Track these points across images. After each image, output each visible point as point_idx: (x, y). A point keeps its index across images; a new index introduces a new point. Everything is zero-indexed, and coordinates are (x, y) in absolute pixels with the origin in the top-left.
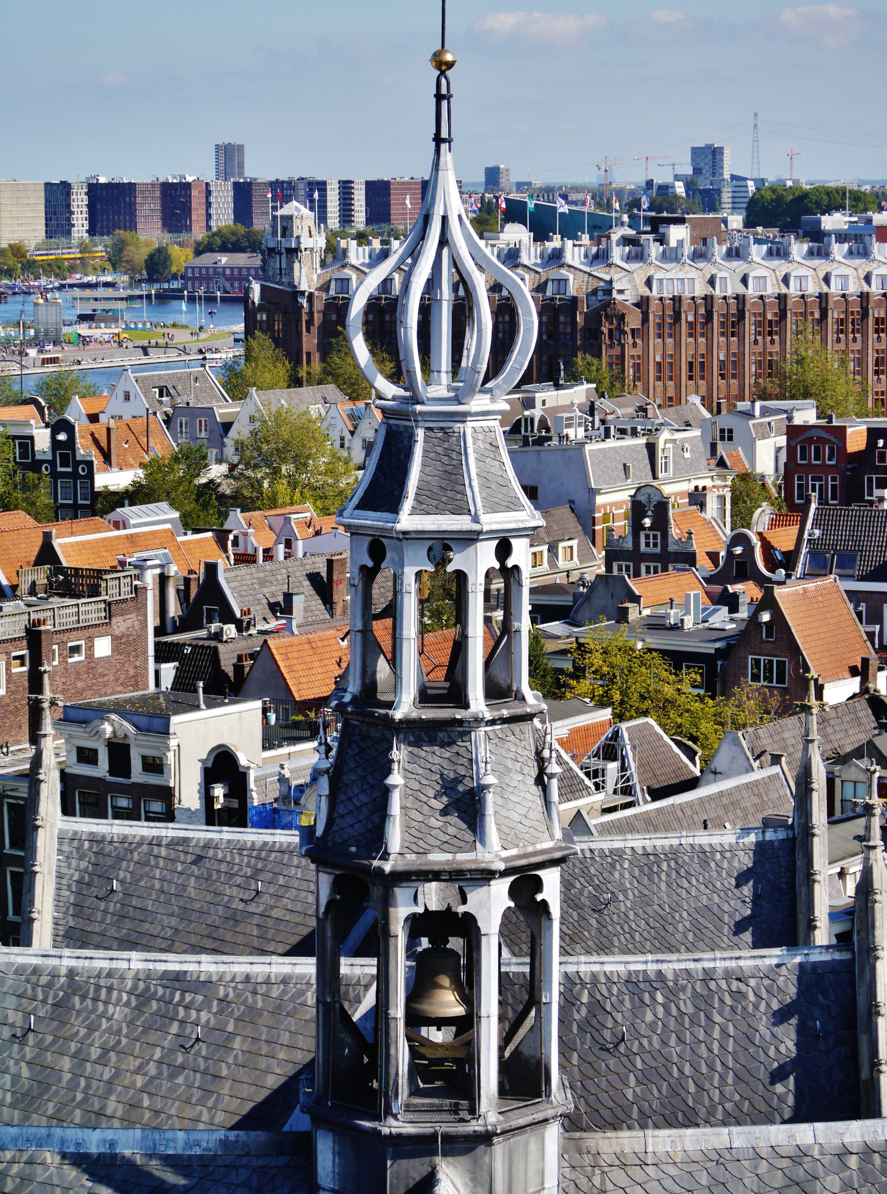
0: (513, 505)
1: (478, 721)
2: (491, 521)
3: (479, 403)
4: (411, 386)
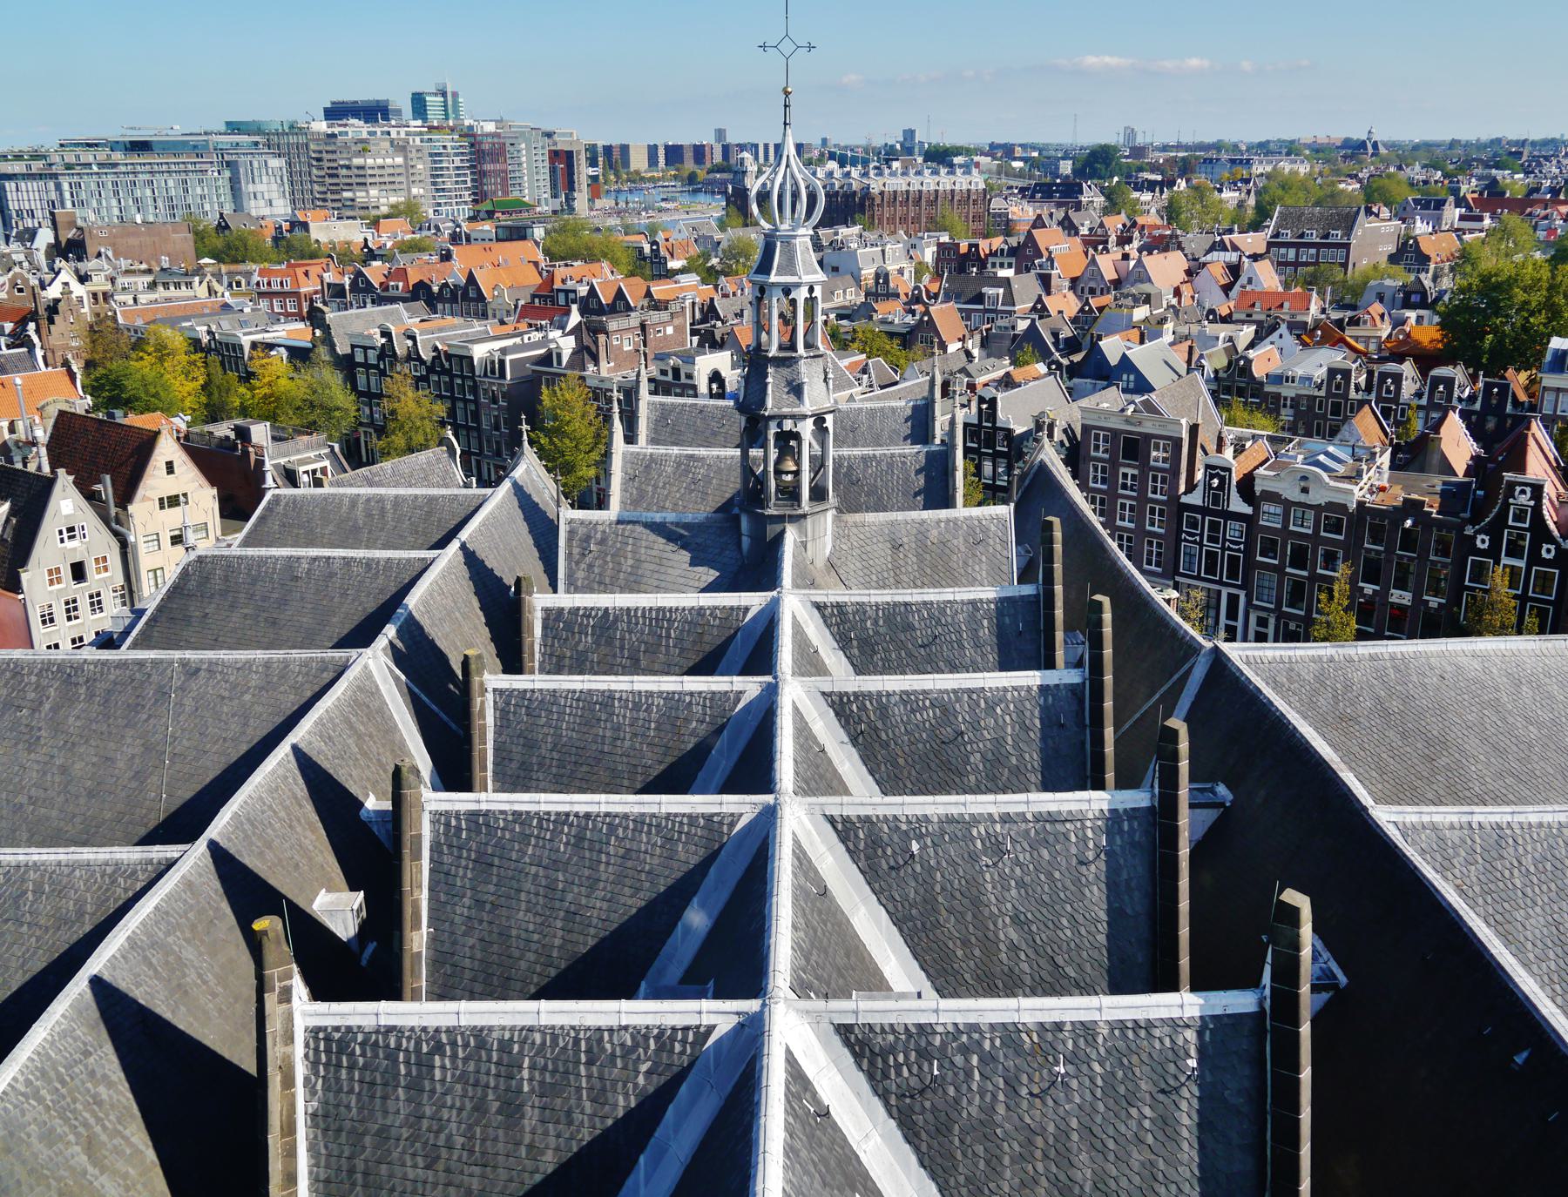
0: (815, 272)
1: (801, 357)
2: (807, 278)
3: (801, 231)
4: (775, 225)
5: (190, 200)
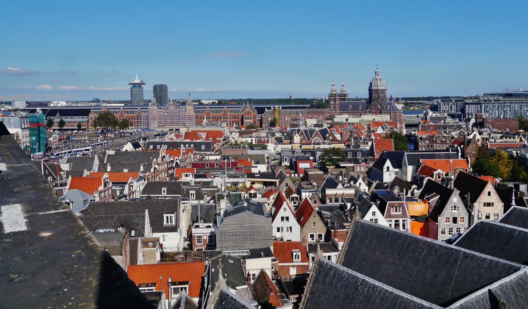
5: (522, 112)
